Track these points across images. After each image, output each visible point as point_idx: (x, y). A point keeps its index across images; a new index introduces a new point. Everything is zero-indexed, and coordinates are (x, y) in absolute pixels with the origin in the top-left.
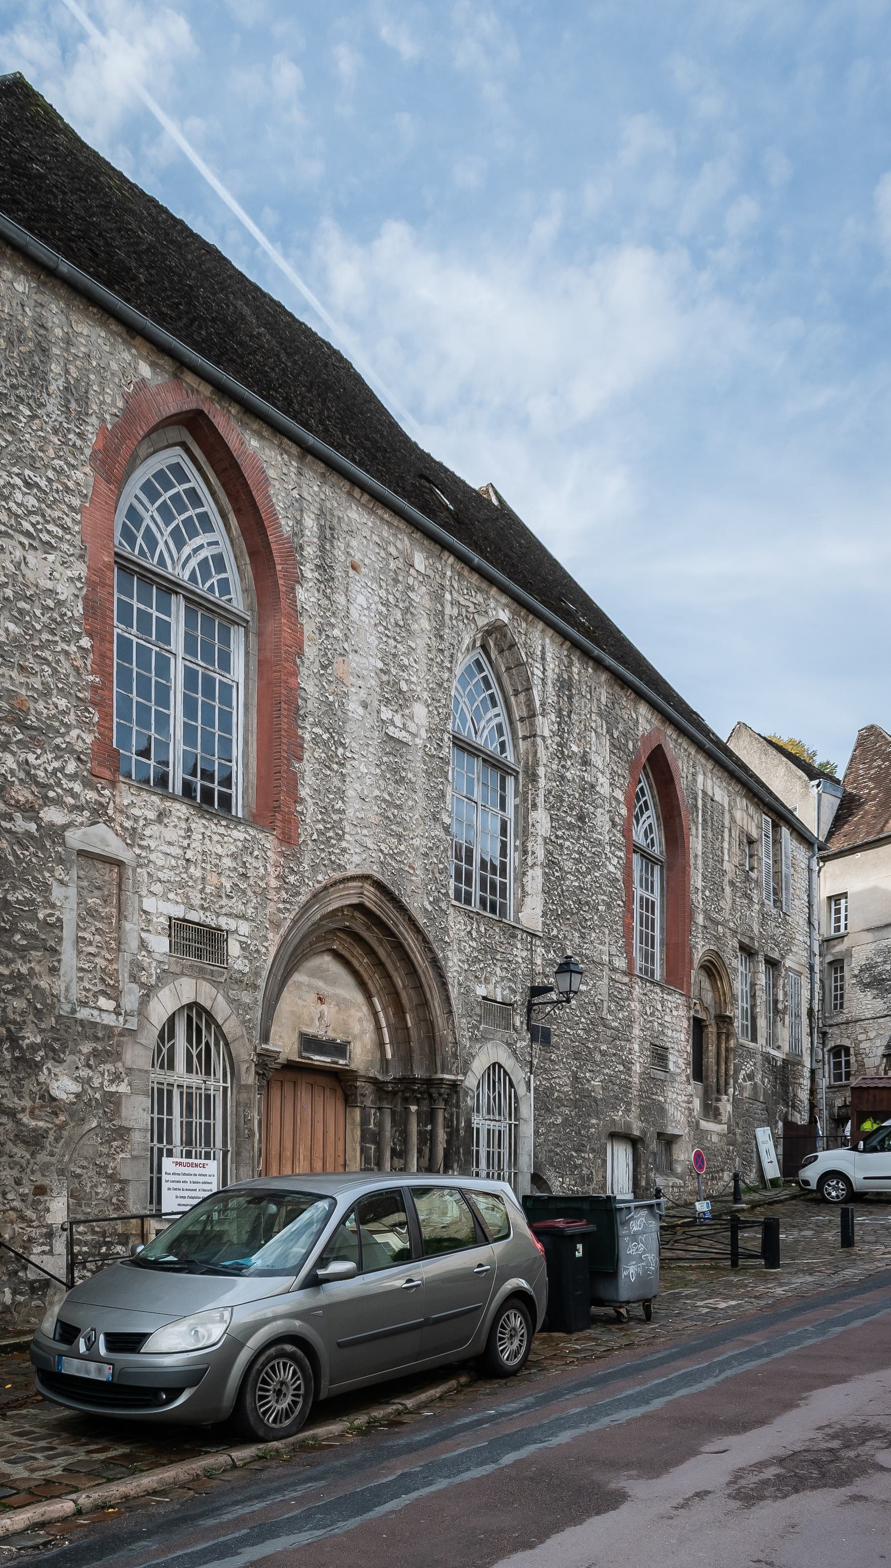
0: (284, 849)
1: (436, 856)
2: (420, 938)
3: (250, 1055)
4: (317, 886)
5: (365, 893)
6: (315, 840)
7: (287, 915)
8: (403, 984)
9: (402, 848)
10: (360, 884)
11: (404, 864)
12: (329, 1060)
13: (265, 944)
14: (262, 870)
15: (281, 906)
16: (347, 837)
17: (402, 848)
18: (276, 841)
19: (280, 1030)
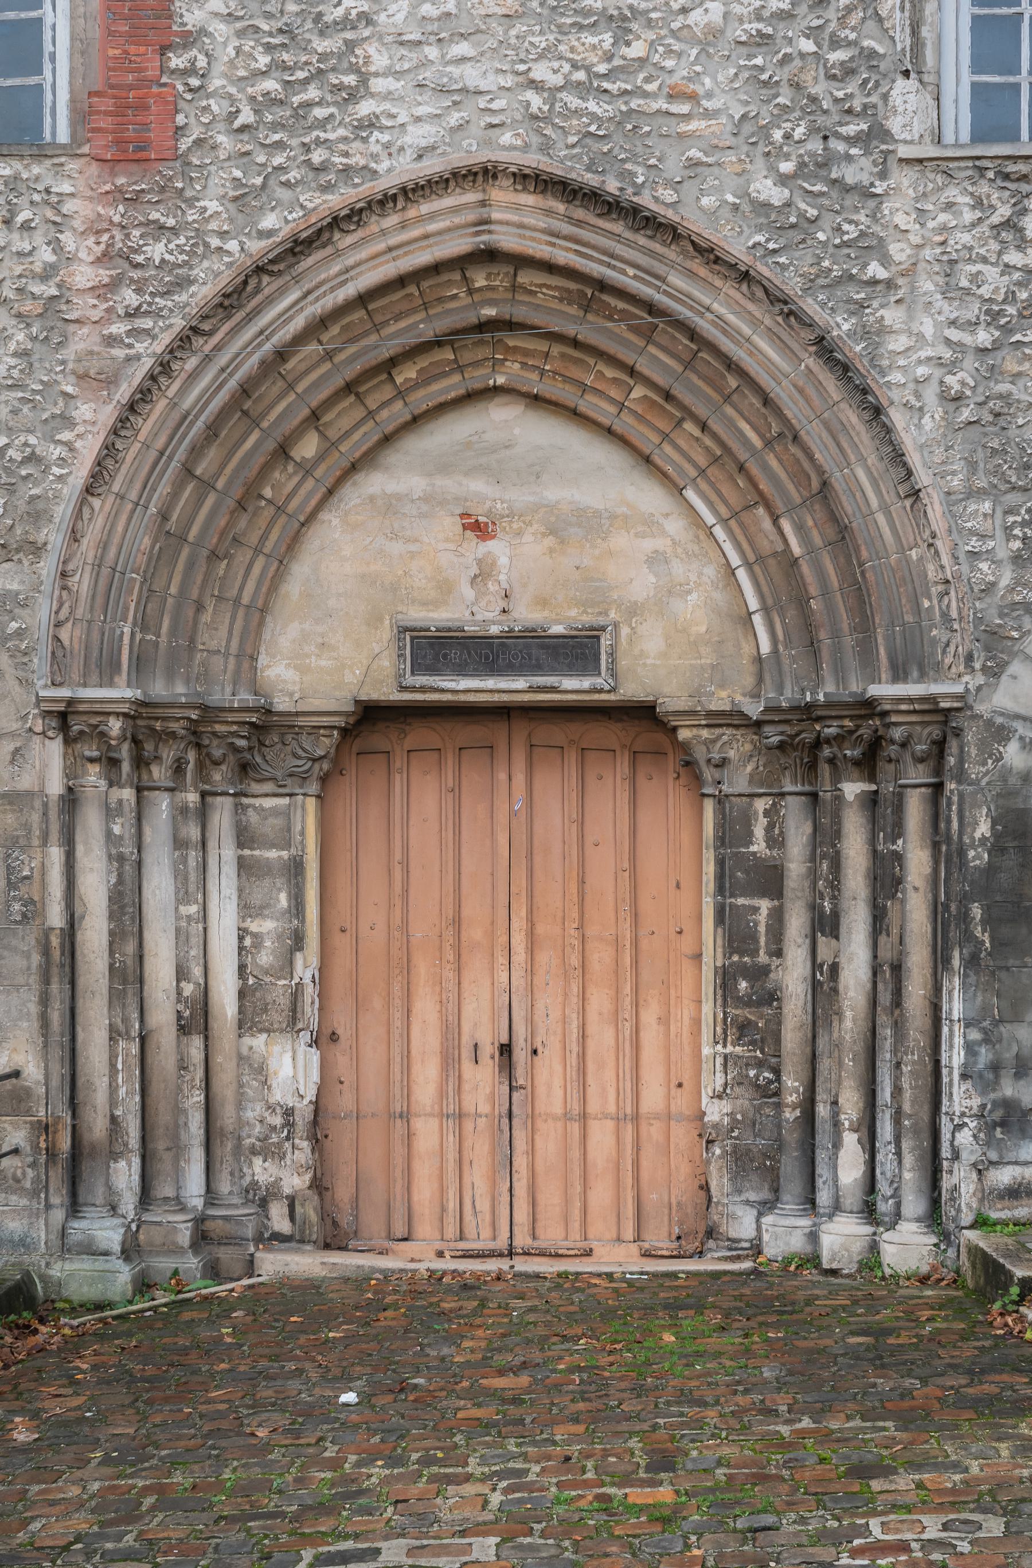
0: (121, 181)
1: (811, 33)
2: (760, 293)
3: (24, 718)
4: (256, 246)
5: (496, 216)
6: (244, 128)
7: (140, 347)
8: (761, 436)
9: (637, 50)
10: (472, 197)
11: (646, 95)
12: (521, 683)
13: (66, 436)
14: (47, 255)
15: (118, 328)
16: (378, 85)
17: (637, 50)
18: (94, 168)
19: (320, 629)
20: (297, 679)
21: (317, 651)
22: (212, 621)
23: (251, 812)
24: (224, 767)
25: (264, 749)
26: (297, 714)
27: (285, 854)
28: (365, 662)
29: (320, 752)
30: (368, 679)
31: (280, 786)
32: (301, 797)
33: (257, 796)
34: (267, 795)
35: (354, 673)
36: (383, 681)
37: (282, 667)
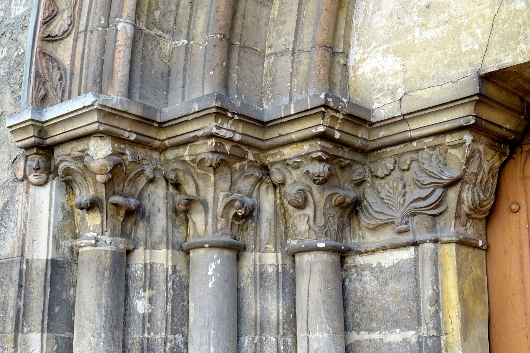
20: (399, 67)
21: (421, 20)
22: (280, 15)
23: (367, 276)
24: (309, 211)
25: (378, 182)
26: (406, 118)
27: (411, 334)
28: (489, 13)
29: (447, 176)
30: (495, 38)
31: (400, 232)
32: (429, 246)
33: (373, 252)
34: (384, 249)
35: (473, 35)
36: (516, 36)
37: (379, 57)
